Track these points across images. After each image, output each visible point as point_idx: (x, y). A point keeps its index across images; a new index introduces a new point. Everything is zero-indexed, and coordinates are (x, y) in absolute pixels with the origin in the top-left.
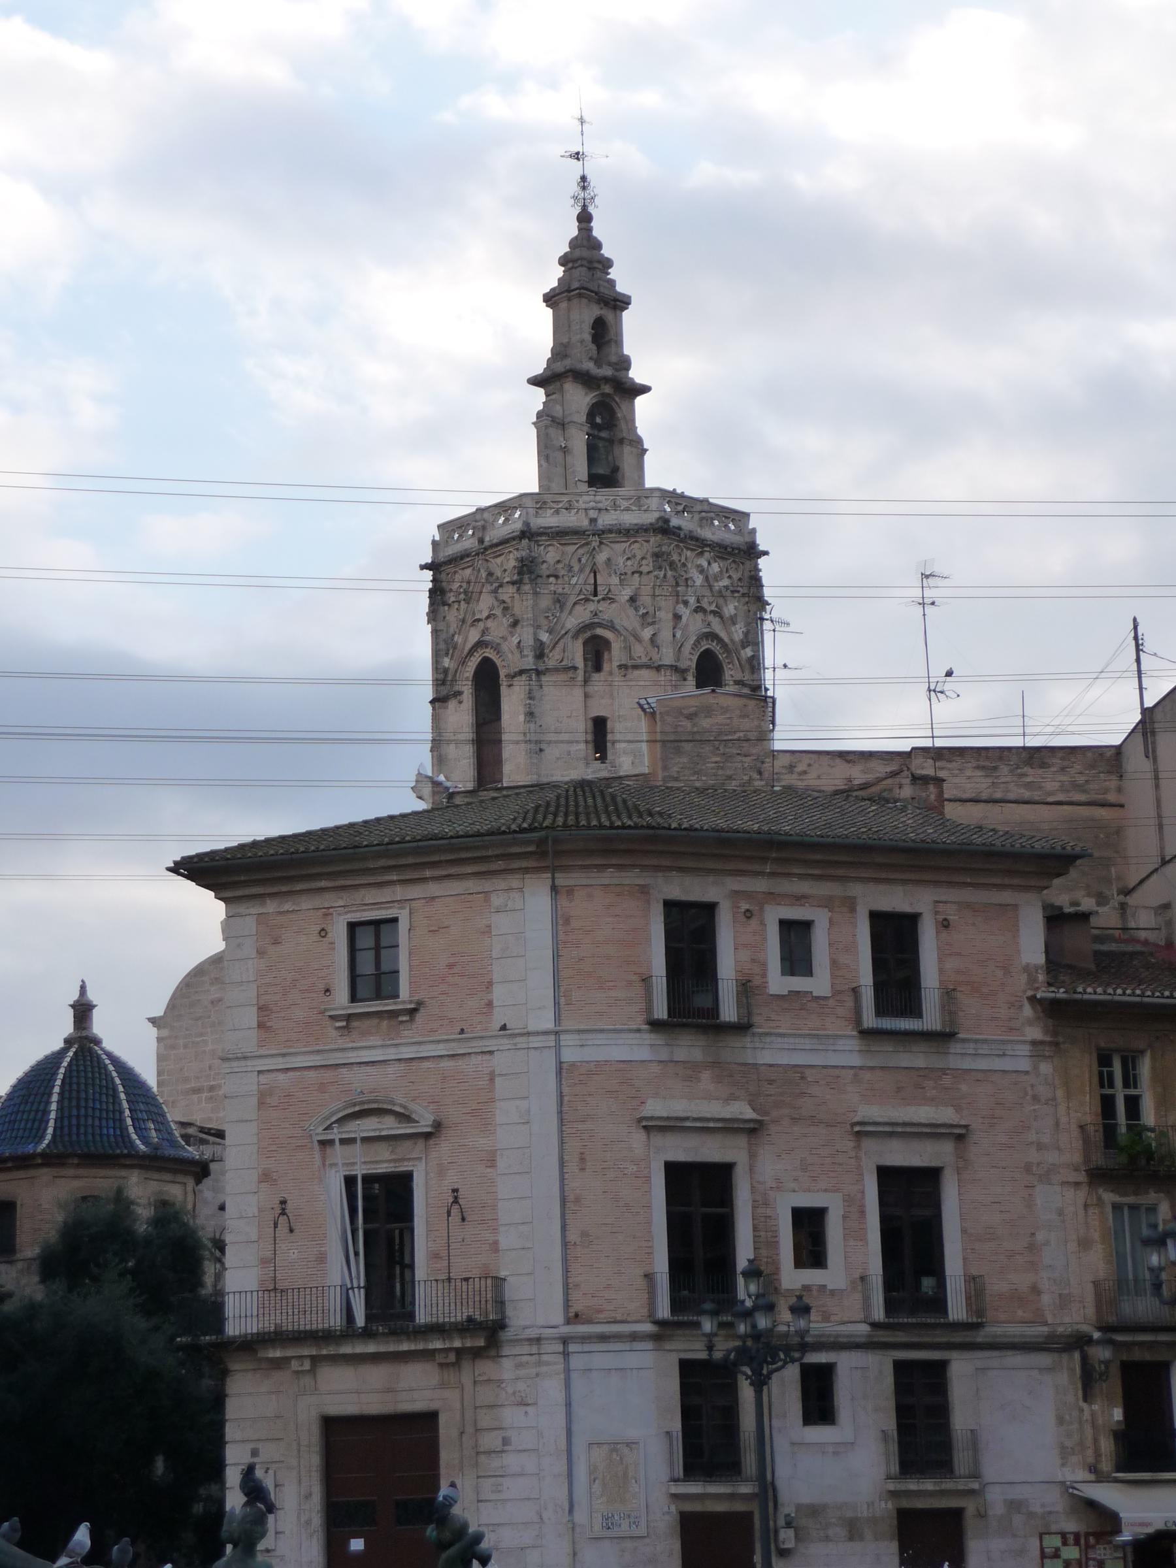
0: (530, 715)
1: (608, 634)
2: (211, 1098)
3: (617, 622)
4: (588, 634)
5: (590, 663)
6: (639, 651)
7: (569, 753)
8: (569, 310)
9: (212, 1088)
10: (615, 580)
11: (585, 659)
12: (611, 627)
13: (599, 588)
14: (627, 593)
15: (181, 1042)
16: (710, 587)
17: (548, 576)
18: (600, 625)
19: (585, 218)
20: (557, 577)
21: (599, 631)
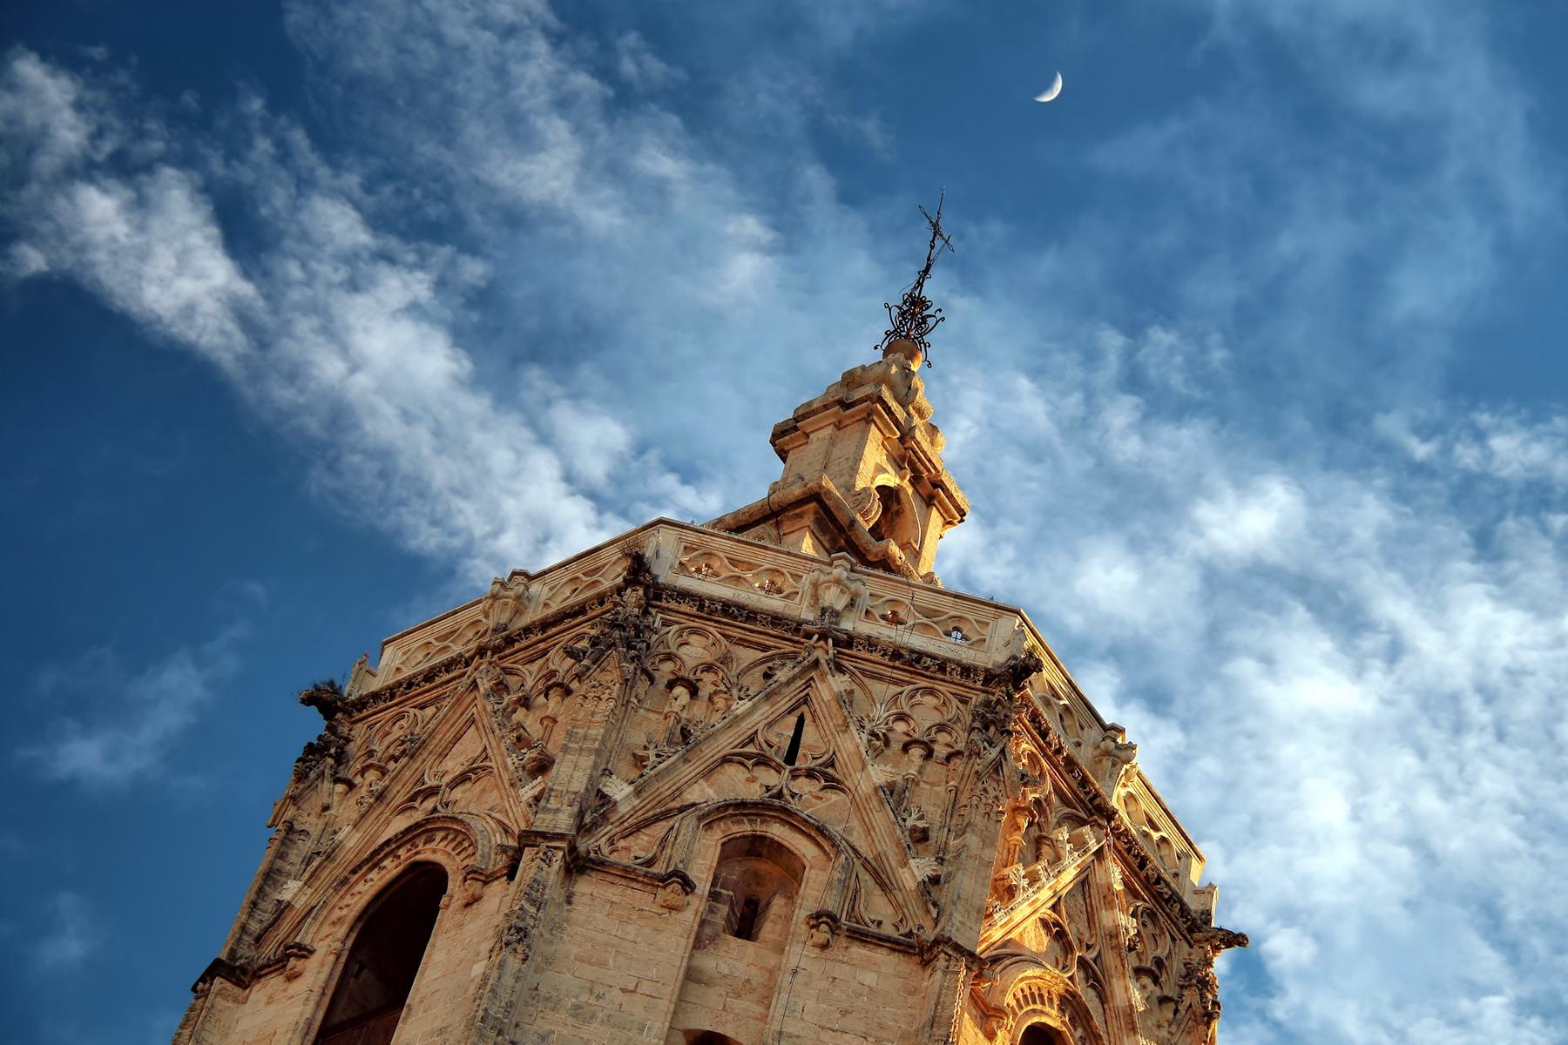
0: (516, 935)
3: (836, 829)
4: (746, 828)
5: (724, 909)
6: (878, 910)
8: (833, 442)
10: (852, 743)
11: (714, 896)
13: (801, 751)
14: (879, 774)
16: (1091, 920)
17: (671, 685)
18: (787, 817)
20: (694, 691)
21: (777, 831)
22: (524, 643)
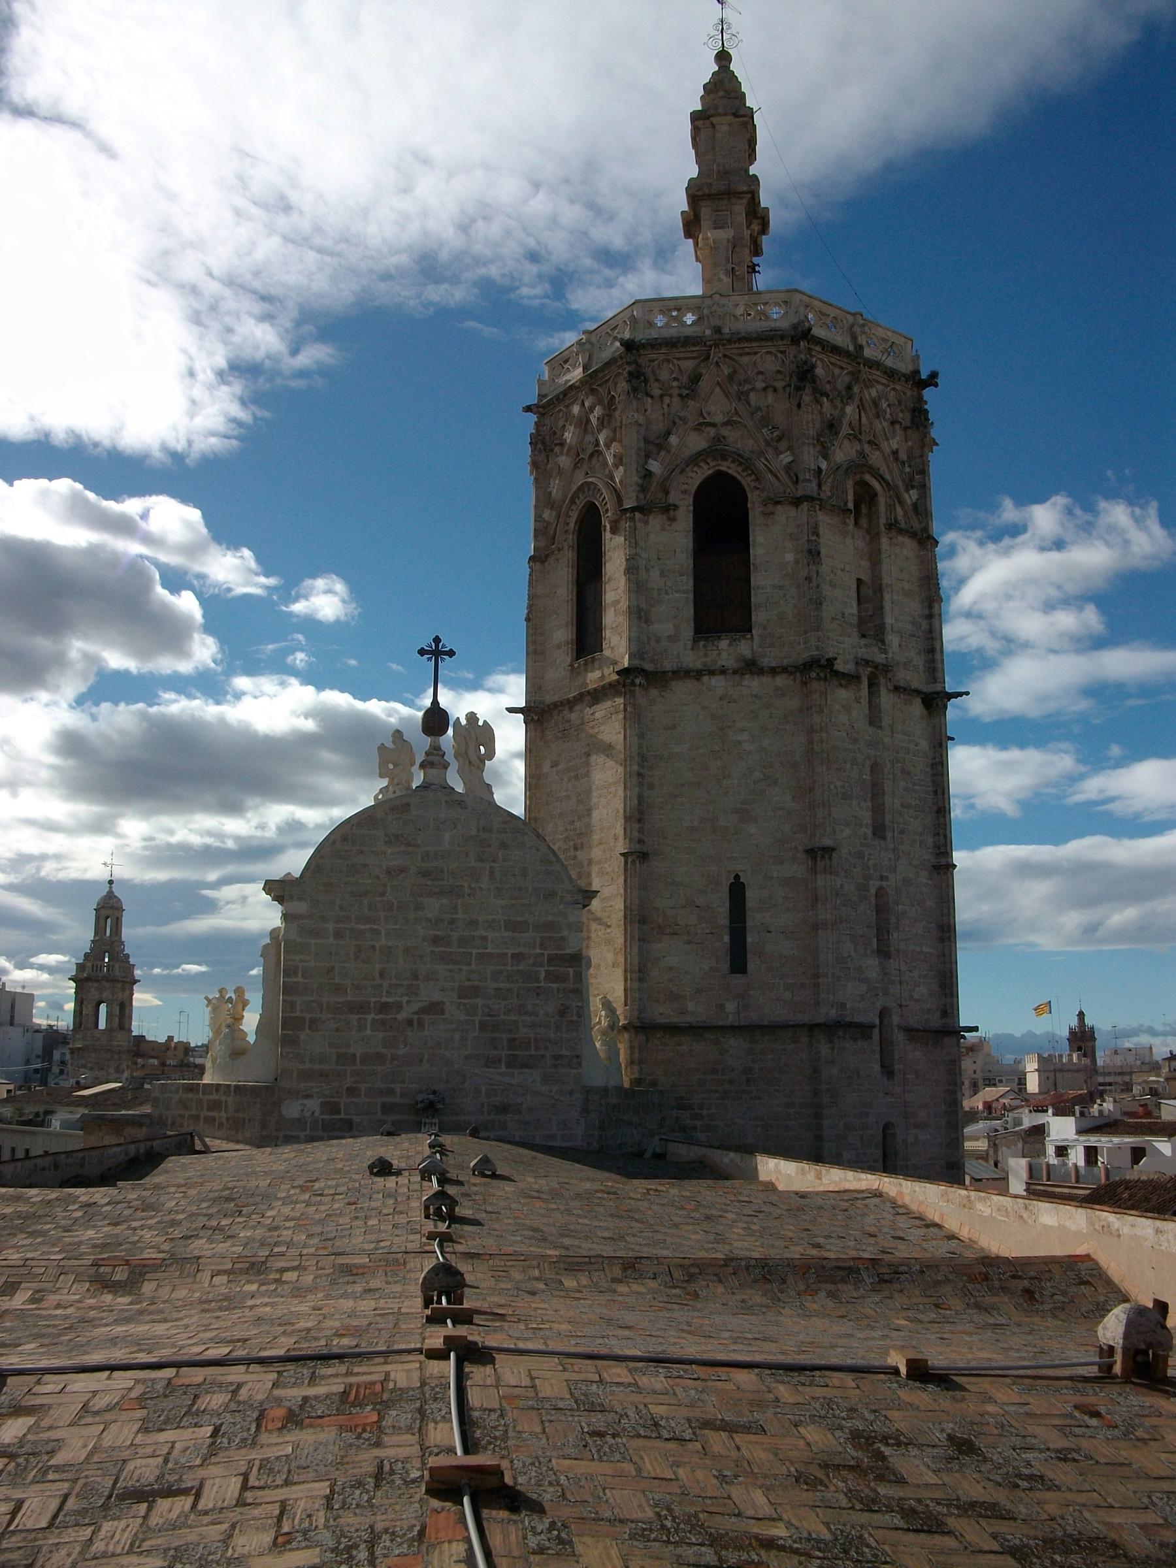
1: (876, 485)
2: (383, 1022)
4: (858, 477)
7: (843, 614)
9: (384, 1008)
12: (881, 478)
15: (331, 927)
19: (723, 57)
22: (737, 345)
